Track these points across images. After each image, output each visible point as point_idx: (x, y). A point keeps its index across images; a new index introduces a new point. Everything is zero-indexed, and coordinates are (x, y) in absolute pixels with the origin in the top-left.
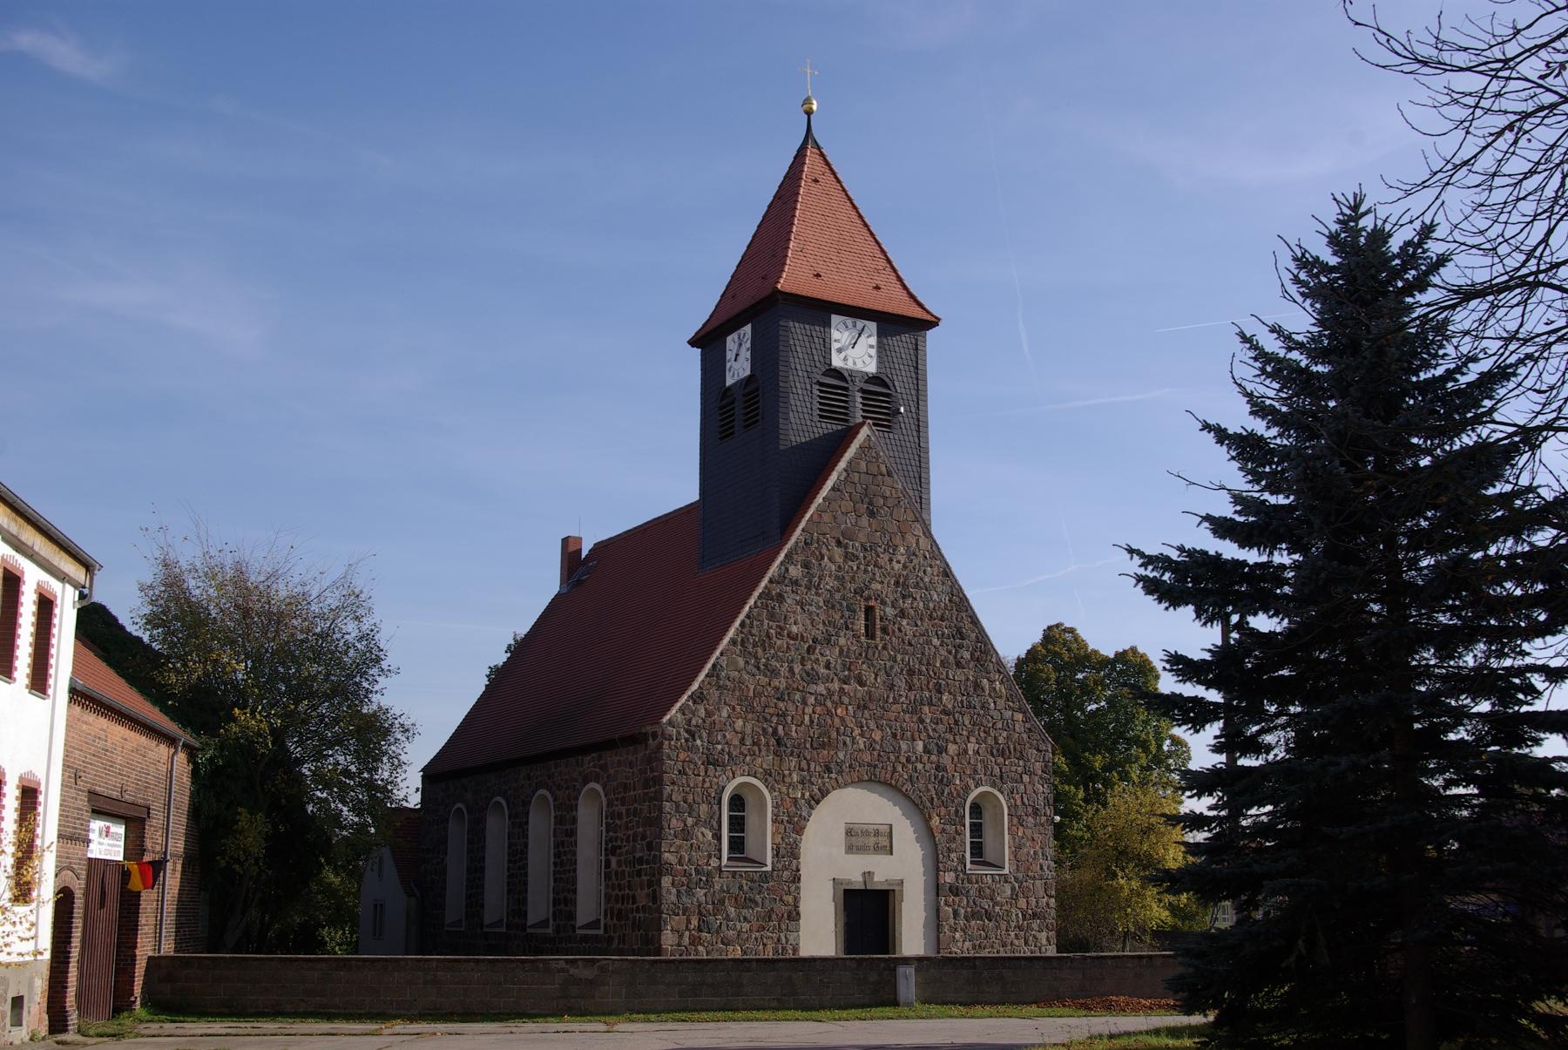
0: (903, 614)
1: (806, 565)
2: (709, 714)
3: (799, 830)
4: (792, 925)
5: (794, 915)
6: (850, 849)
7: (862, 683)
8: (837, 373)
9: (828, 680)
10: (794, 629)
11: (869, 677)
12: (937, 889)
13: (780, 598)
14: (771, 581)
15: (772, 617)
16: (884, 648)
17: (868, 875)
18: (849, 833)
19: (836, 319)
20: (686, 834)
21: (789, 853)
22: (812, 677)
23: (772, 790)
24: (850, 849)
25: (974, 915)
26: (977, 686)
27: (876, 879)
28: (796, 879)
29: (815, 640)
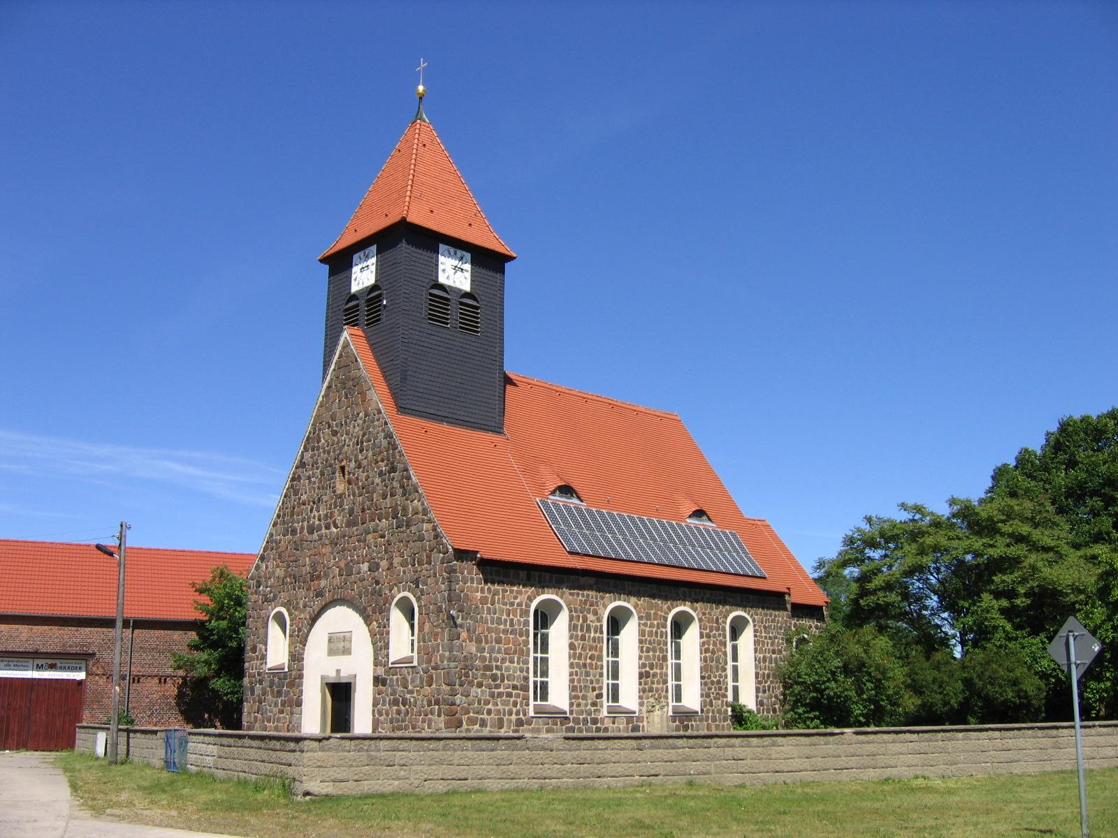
0: (359, 466)
1: (313, 450)
2: (267, 568)
3: (304, 642)
4: (296, 709)
5: (299, 704)
6: (332, 652)
7: (336, 527)
8: (354, 297)
9: (319, 529)
10: (304, 497)
11: (339, 519)
12: (378, 681)
13: (299, 477)
14: (296, 468)
15: (296, 493)
16: (349, 496)
17: (338, 671)
18: (330, 640)
19: (355, 257)
20: (254, 650)
21: (296, 658)
22: (311, 532)
23: (290, 614)
24: (332, 652)
25: (395, 702)
26: (405, 509)
27: (342, 674)
28: (301, 677)
29: (314, 503)
